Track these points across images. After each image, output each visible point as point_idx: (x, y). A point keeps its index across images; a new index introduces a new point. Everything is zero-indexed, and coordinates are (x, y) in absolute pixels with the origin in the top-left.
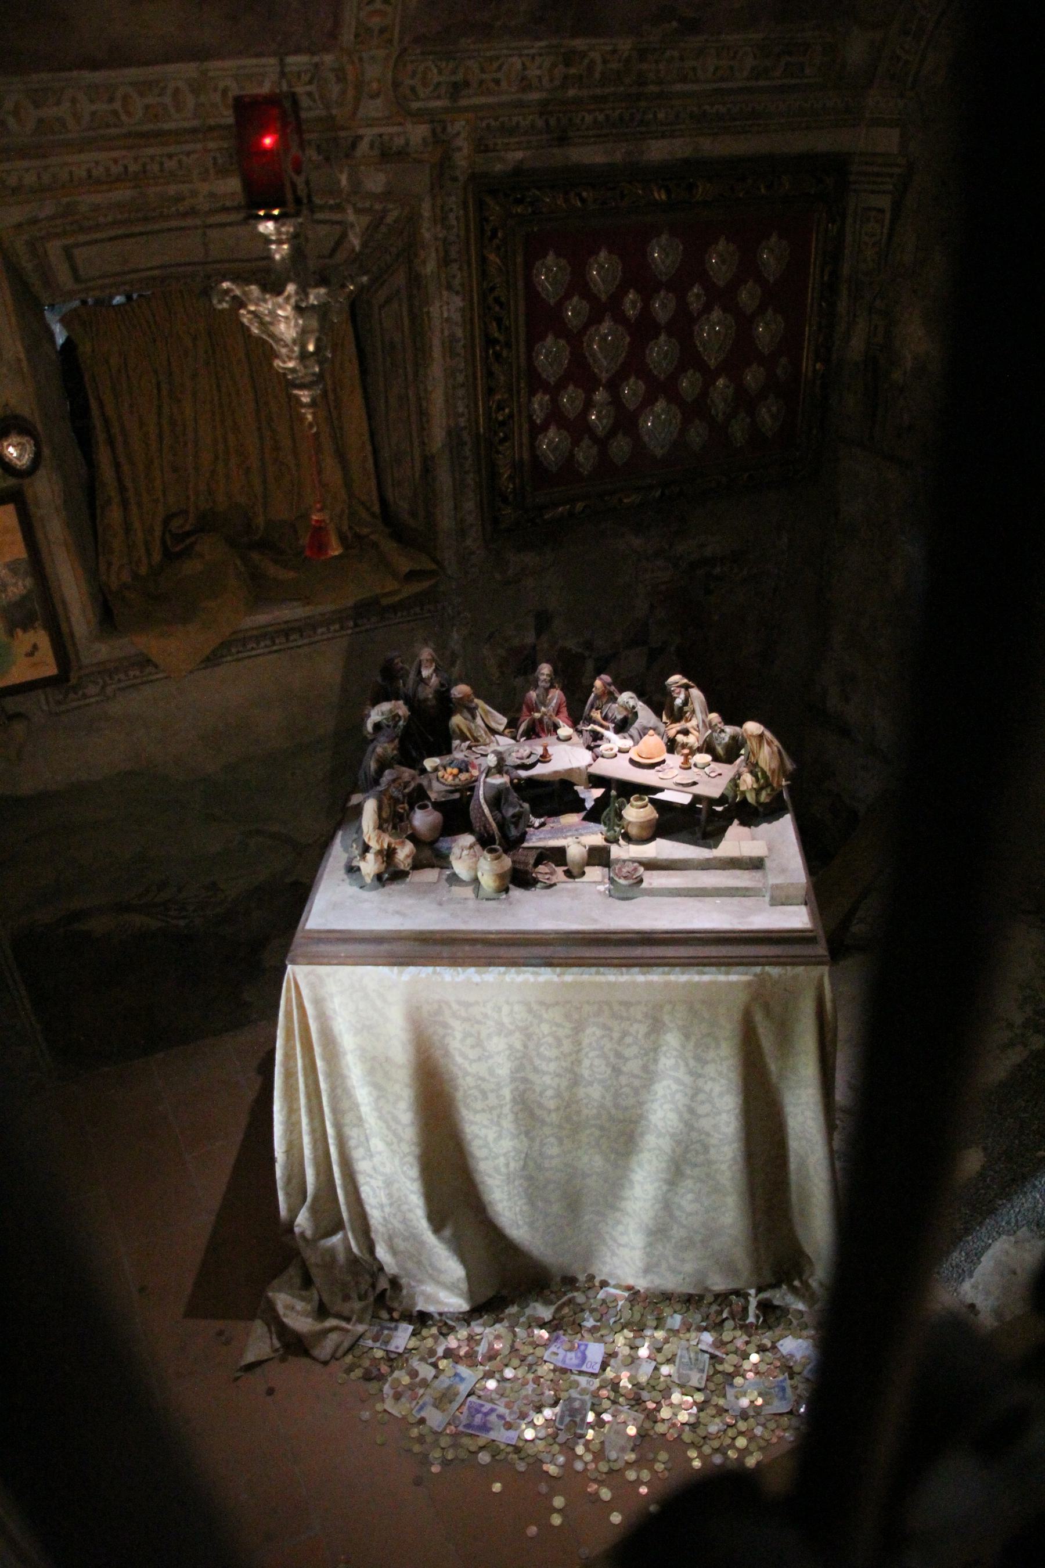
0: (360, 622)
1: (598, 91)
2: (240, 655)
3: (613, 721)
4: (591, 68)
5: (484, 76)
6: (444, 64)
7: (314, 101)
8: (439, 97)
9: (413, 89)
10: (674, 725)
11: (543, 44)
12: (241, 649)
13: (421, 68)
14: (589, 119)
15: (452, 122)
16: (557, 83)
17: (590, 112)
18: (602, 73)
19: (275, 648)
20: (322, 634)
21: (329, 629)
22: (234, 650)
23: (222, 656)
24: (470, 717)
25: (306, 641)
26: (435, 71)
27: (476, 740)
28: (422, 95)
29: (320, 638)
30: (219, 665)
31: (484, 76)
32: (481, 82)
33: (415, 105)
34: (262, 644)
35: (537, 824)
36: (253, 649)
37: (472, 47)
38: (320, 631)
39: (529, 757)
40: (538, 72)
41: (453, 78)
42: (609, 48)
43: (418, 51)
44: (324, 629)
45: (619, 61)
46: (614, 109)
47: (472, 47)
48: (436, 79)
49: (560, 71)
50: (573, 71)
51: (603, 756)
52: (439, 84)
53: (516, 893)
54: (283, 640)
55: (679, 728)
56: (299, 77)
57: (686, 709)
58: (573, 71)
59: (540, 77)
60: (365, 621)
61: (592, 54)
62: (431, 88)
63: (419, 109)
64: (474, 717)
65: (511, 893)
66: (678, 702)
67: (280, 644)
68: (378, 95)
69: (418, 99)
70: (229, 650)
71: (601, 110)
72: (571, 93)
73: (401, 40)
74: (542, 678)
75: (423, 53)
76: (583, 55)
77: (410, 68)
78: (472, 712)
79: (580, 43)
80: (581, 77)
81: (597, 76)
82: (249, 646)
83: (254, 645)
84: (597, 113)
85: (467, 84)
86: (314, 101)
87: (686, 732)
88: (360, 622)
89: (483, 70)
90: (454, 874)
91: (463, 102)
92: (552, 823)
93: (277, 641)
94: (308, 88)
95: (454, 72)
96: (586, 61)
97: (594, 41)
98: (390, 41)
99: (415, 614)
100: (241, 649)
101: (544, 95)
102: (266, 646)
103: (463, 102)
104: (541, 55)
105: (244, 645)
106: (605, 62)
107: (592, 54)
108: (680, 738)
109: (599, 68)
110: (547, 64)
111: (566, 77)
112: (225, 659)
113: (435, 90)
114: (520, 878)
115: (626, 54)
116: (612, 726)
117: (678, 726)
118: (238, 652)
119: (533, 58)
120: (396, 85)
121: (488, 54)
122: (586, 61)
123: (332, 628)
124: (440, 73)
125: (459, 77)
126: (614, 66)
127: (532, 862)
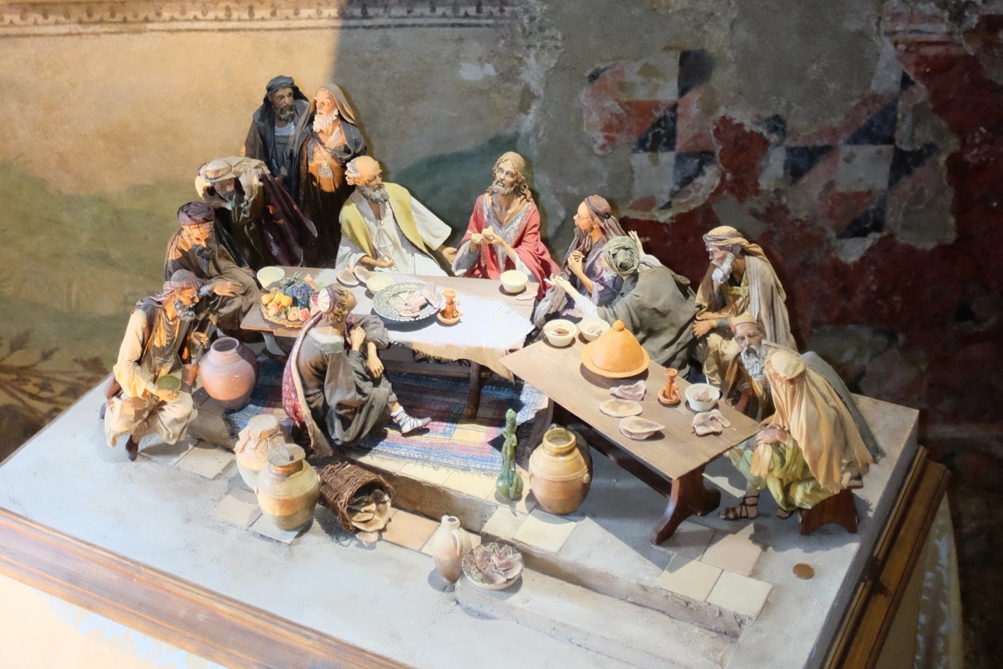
0: (371, 11)
2: (174, 25)
3: (601, 281)
10: (710, 315)
12: (177, 15)
19: (229, 25)
20: (309, 18)
21: (319, 13)
22: (166, 15)
23: (147, 20)
24: (372, 214)
25: (282, 24)
27: (375, 254)
30: (139, 32)
34: (211, 15)
35: (406, 429)
36: (196, 19)
38: (305, 12)
39: (423, 307)
44: (312, 12)
51: (547, 341)
53: (317, 540)
54: (245, 16)
55: (715, 323)
57: (736, 290)
60: (381, 11)
64: (378, 217)
65: (307, 537)
66: (718, 275)
67: (239, 20)
70: (159, 14)
74: (500, 176)
78: (378, 207)
82: (190, 15)
83: (200, 16)
87: (725, 332)
88: (371, 11)
90: (239, 477)
92: (440, 433)
93: (235, 15)
99: (466, 16)
102: (217, 19)
108: (714, 339)
112: (150, 26)
114: (329, 515)
116: (596, 287)
117: (713, 319)
118: (173, 19)
123: (326, 12)
127: (347, 495)
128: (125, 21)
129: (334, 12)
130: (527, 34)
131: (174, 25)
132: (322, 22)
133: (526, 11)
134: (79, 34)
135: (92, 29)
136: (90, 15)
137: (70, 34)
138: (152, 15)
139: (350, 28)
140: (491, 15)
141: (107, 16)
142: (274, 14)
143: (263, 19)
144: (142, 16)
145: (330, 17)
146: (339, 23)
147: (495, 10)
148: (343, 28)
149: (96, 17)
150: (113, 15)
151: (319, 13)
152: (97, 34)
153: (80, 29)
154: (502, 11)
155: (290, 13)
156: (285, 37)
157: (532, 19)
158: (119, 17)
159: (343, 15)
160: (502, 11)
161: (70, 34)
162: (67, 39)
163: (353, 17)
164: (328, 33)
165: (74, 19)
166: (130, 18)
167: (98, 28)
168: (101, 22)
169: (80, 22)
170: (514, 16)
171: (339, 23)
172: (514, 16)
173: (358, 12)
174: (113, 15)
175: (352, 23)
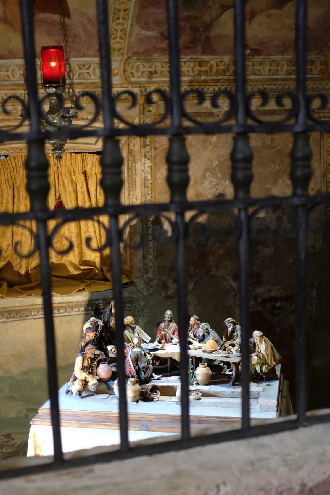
1: (215, 77)
2: (35, 317)
4: (211, 66)
5: (164, 69)
6: (146, 64)
7: (90, 76)
8: (144, 77)
9: (132, 73)
11: (188, 57)
12: (36, 313)
13: (136, 65)
14: (211, 89)
15: (149, 87)
16: (196, 73)
17: (211, 86)
18: (217, 70)
20: (76, 311)
21: (79, 309)
22: (33, 314)
23: (27, 316)
25: (68, 314)
26: (142, 66)
28: (136, 76)
29: (74, 313)
30: (25, 320)
31: (164, 69)
32: (162, 72)
33: (133, 80)
37: (158, 57)
38: (74, 310)
40: (188, 69)
41: (150, 70)
42: (220, 60)
43: (135, 58)
44: (77, 309)
45: (224, 65)
46: (222, 86)
47: (158, 57)
48: (142, 70)
49: (197, 68)
50: (203, 69)
52: (143, 72)
56: (84, 66)
58: (203, 69)
59: (188, 71)
61: (211, 62)
62: (140, 73)
63: (135, 82)
68: (117, 75)
69: (134, 78)
70: (31, 314)
71: (216, 86)
72: (203, 78)
73: (127, 54)
75: (137, 59)
76: (207, 62)
77: (131, 64)
79: (206, 58)
80: (207, 71)
81: (214, 71)
84: (215, 87)
85: (156, 72)
86: (90, 76)
89: (163, 67)
91: (154, 79)
94: (88, 71)
95: (150, 67)
96: (209, 65)
97: (212, 57)
98: (123, 54)
100: (36, 313)
101: (190, 78)
103: (154, 79)
104: (188, 62)
105: (38, 312)
106: (217, 66)
107: (211, 62)
109: (215, 67)
110: (192, 65)
111: (200, 71)
112: (28, 318)
113: (142, 74)
115: (227, 63)
118: (35, 315)
119: (185, 62)
120: (125, 71)
121: (165, 60)
122: (209, 65)
124: (144, 67)
125: (152, 69)
126: (222, 67)
128: (20, 316)
129: (83, 309)
130: (139, 312)
131: (35, 317)
132: (80, 313)
133: (139, 305)
134: (6, 322)
135: (10, 320)
136: (10, 315)
137: (3, 322)
138: (29, 314)
139: (88, 314)
140: (128, 307)
141: (15, 315)
142: (65, 311)
143: (62, 313)
144: (25, 315)
145: (82, 311)
146: (84, 313)
147: (130, 305)
148: (86, 314)
149: (12, 316)
150: (17, 315)
151: (79, 309)
152: (12, 321)
153: (7, 320)
154: (132, 305)
155: (70, 310)
156: (69, 318)
157: (140, 307)
158: (19, 315)
159: (86, 310)
160: (132, 305)
161: (3, 322)
162: (3, 324)
163: (89, 310)
164: (81, 316)
165: (5, 317)
166: (22, 315)
167: (12, 319)
168: (13, 317)
169: (7, 318)
170: (135, 306)
171: (84, 313)
172: (135, 306)
173: (90, 309)
174: (17, 315)
175: (89, 312)
